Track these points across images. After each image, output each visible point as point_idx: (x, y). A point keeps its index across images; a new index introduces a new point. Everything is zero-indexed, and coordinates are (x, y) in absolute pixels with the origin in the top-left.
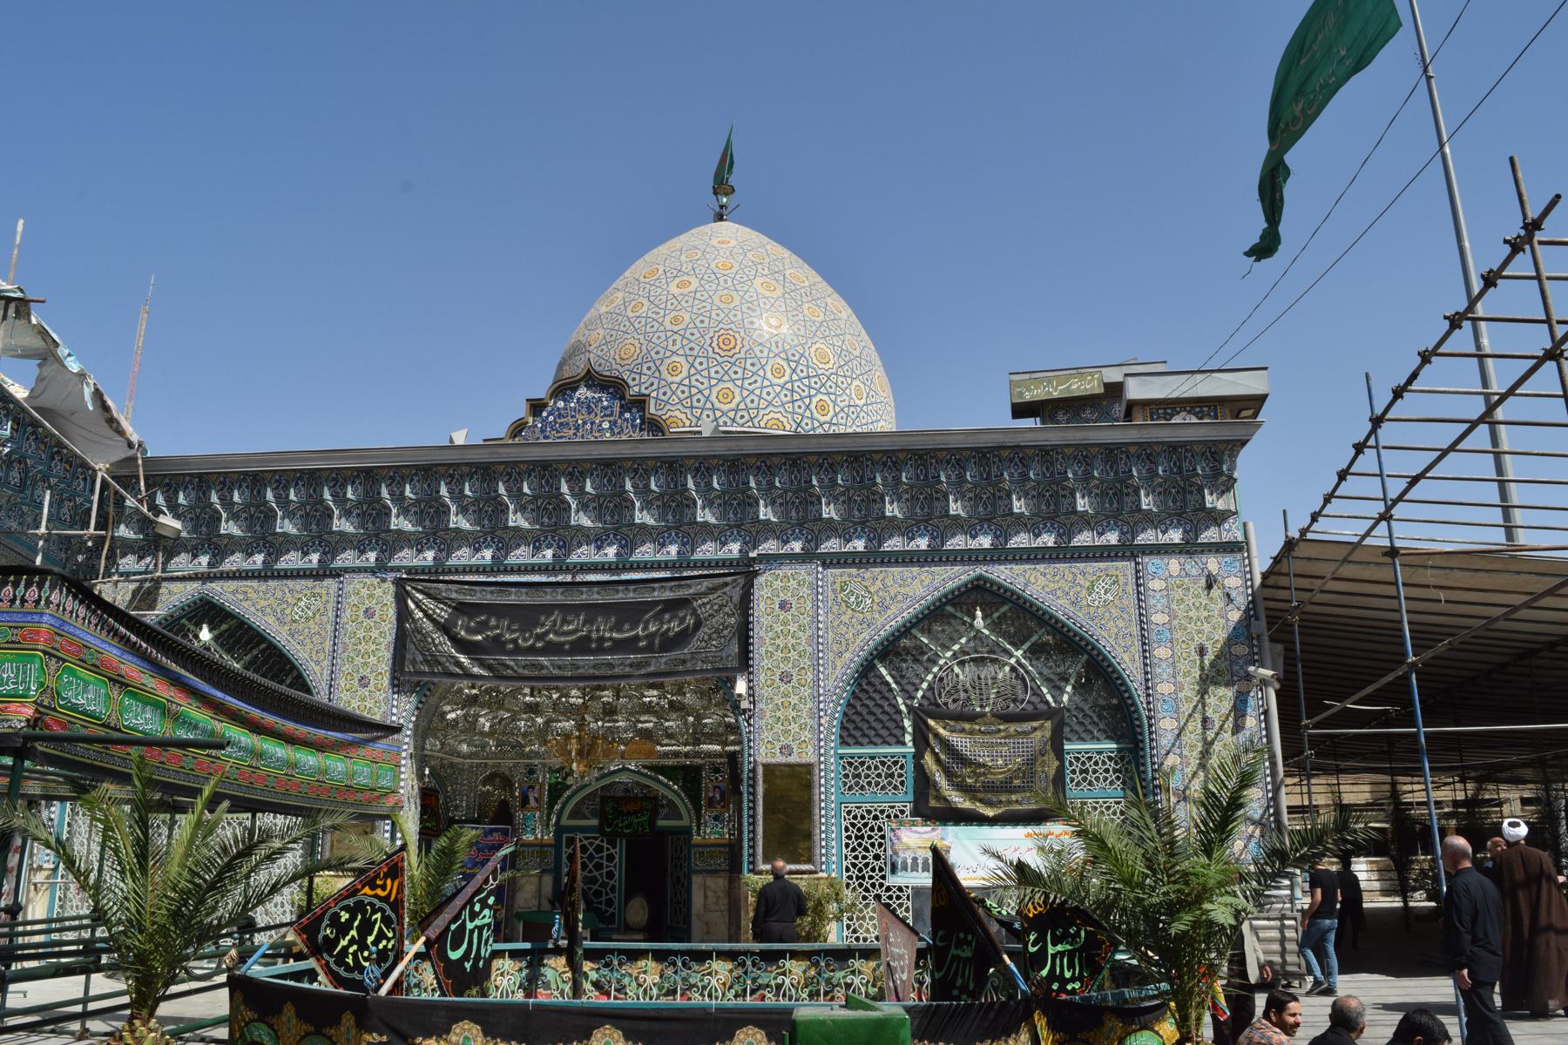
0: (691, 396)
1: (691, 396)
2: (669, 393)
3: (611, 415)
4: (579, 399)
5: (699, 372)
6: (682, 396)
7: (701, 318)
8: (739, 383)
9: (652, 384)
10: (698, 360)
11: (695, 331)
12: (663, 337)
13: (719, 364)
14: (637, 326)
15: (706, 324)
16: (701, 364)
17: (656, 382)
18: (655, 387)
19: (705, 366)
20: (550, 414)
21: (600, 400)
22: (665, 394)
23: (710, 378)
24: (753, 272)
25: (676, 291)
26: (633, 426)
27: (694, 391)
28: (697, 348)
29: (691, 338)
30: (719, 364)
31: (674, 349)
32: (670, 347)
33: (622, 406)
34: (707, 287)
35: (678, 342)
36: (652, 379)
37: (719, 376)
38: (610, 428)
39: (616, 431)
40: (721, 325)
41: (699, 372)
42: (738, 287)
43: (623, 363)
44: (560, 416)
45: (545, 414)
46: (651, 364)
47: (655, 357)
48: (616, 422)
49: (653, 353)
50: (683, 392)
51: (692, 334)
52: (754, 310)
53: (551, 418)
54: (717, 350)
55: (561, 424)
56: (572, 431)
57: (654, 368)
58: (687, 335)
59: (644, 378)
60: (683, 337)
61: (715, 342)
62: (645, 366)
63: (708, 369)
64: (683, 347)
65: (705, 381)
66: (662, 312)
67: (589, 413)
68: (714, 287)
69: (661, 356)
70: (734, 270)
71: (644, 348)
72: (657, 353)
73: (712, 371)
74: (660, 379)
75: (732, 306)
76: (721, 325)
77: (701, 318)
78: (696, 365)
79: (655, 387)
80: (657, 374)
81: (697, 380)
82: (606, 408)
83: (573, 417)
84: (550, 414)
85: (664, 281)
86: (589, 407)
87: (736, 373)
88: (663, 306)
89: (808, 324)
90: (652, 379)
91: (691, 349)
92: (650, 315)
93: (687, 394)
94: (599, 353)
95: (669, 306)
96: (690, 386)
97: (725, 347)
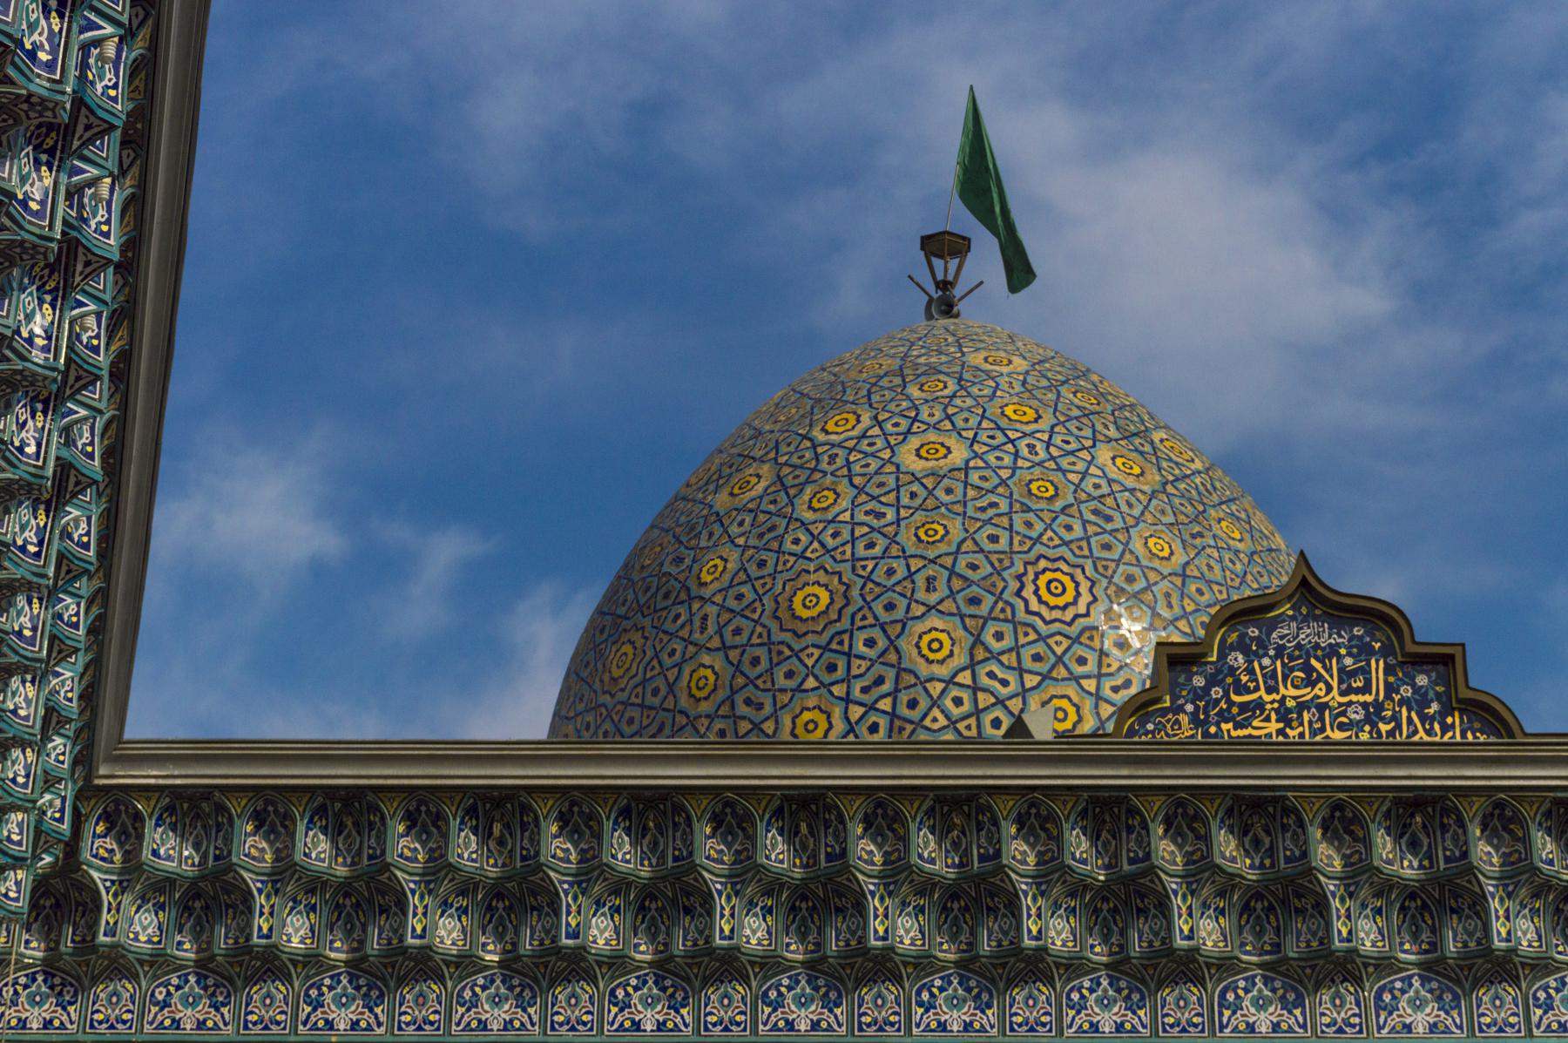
0: (978, 712)
1: (978, 712)
2: (924, 703)
3: (1366, 689)
4: (1280, 650)
5: (995, 656)
6: (956, 712)
7: (990, 530)
8: (1090, 685)
9: (880, 681)
10: (992, 628)
11: (979, 559)
12: (901, 573)
13: (1042, 638)
14: (830, 543)
15: (1003, 543)
16: (999, 636)
17: (890, 674)
18: (887, 687)
19: (1007, 642)
20: (1212, 681)
21: (1333, 651)
22: (913, 704)
23: (1021, 671)
24: (1088, 432)
25: (918, 466)
26: (1424, 718)
27: (984, 700)
28: (988, 600)
29: (969, 573)
30: (1042, 638)
31: (933, 598)
32: (921, 595)
33: (1389, 670)
34: (991, 458)
35: (941, 585)
36: (878, 669)
37: (1043, 667)
38: (1368, 720)
39: (1384, 728)
40: (1039, 549)
41: (995, 656)
42: (1064, 463)
43: (802, 628)
44: (1241, 689)
45: (1199, 681)
46: (876, 633)
47: (884, 616)
48: (1379, 706)
49: (878, 608)
50: (958, 702)
51: (974, 567)
52: (1109, 519)
53: (1216, 692)
54: (1034, 605)
55: (1243, 707)
56: (1274, 726)
57: (882, 643)
58: (961, 566)
59: (858, 667)
60: (952, 572)
61: (1030, 588)
62: (860, 637)
63: (1016, 649)
64: (952, 594)
65: (1011, 677)
66: (890, 515)
67: (1313, 684)
68: (1008, 460)
69: (899, 613)
70: (1044, 424)
71: (855, 593)
72: (890, 607)
73: (1027, 653)
74: (900, 671)
75: (1058, 505)
76: (1039, 549)
77: (990, 530)
78: (988, 638)
79: (887, 687)
80: (892, 657)
81: (991, 675)
82: (1353, 674)
83: (1269, 691)
84: (1212, 681)
85: (880, 443)
86: (1308, 669)
87: (1082, 661)
88: (891, 498)
89: (1227, 556)
90: (878, 669)
91: (975, 601)
92: (861, 517)
93: (967, 707)
94: (732, 603)
95: (905, 500)
96: (975, 689)
97: (1052, 601)
